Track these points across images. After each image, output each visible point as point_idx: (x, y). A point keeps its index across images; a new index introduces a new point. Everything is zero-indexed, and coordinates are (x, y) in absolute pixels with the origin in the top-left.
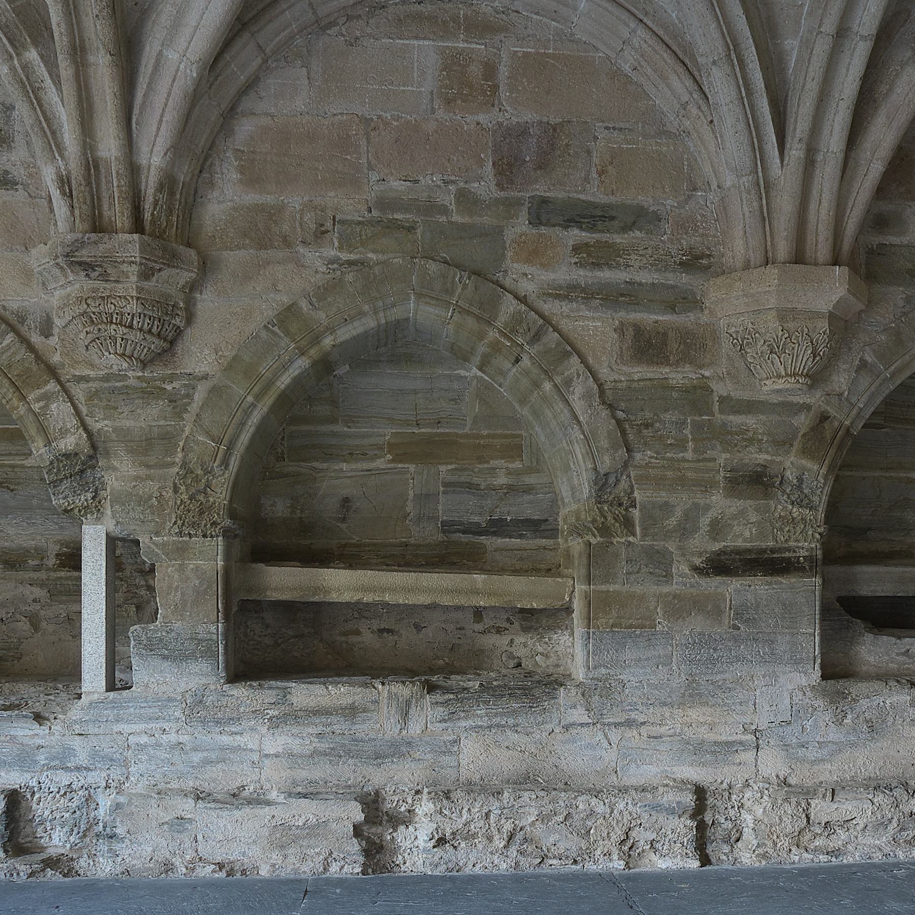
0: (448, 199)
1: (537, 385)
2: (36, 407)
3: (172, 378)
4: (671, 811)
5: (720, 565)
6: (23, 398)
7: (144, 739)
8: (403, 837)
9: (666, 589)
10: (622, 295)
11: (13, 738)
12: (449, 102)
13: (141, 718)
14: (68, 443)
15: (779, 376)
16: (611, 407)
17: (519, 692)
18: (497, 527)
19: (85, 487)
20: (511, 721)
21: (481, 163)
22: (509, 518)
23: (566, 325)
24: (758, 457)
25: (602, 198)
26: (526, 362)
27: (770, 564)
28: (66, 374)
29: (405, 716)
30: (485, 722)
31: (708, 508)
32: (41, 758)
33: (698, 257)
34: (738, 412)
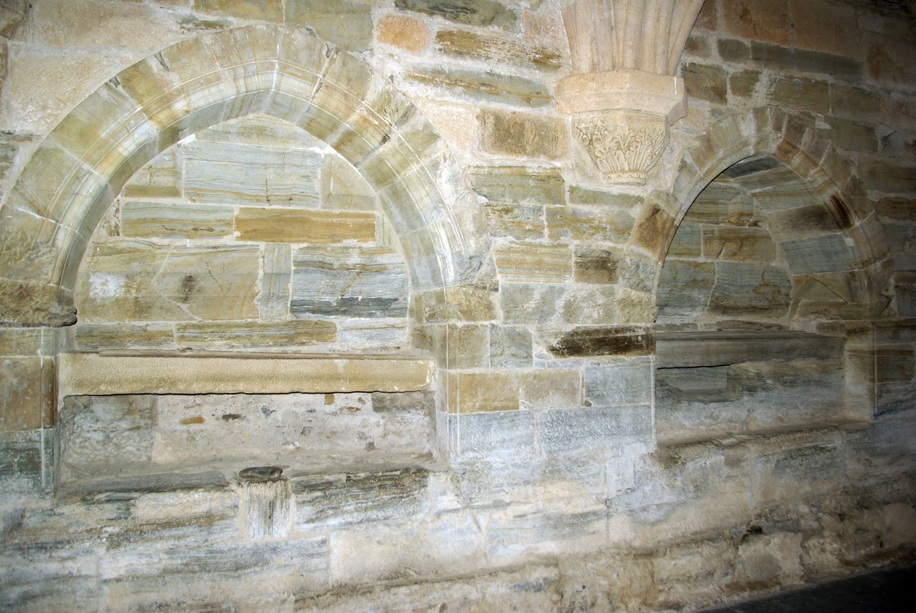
4: (538, 588)
5: (573, 346)
9: (526, 370)
10: (484, 85)
15: (623, 171)
17: (389, 483)
20: (381, 514)
22: (360, 298)
24: (601, 244)
27: (614, 343)
29: (269, 517)
30: (357, 517)
31: (562, 291)
33: (549, 57)
34: (585, 202)
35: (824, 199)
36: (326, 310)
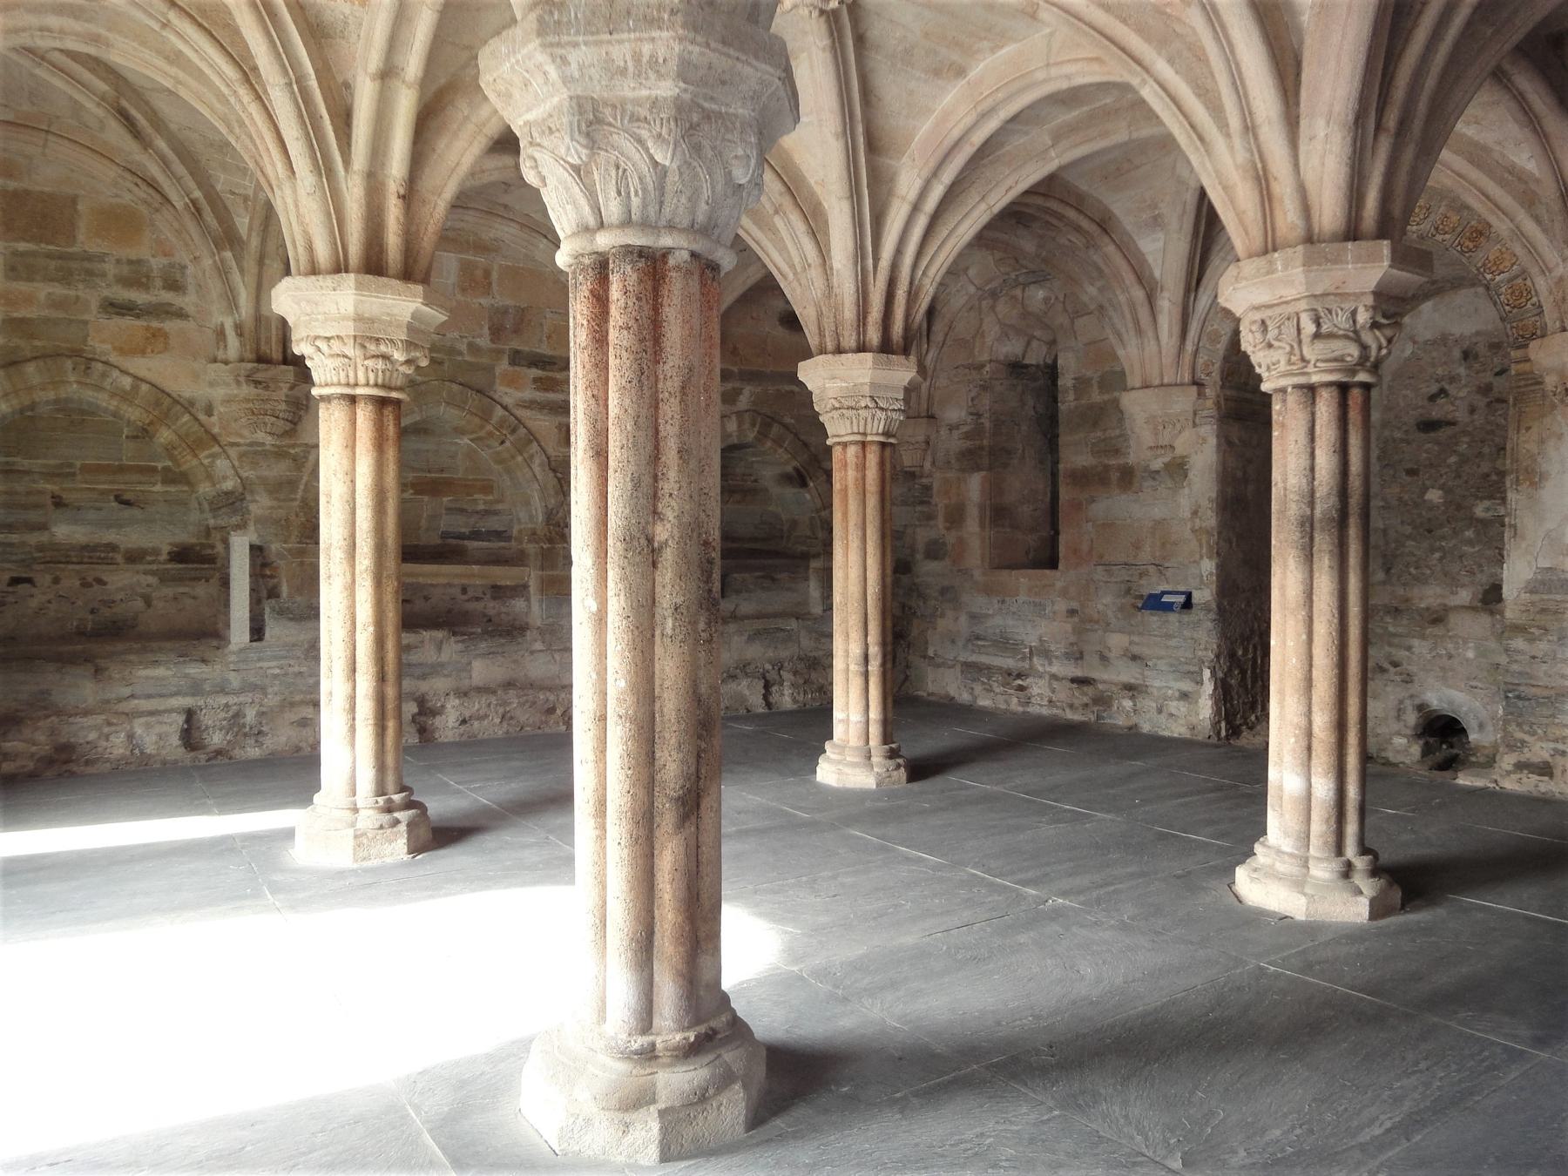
0: (463, 347)
1: (513, 457)
2: (206, 462)
3: (293, 446)
6: (196, 456)
7: (277, 671)
8: (438, 721)
11: (186, 676)
12: (464, 290)
13: (275, 658)
14: (229, 485)
16: (554, 471)
18: (476, 535)
19: (235, 512)
21: (481, 327)
23: (530, 424)
25: (549, 352)
26: (508, 444)
28: (224, 440)
32: (207, 687)
35: (789, 469)
36: (461, 537)
